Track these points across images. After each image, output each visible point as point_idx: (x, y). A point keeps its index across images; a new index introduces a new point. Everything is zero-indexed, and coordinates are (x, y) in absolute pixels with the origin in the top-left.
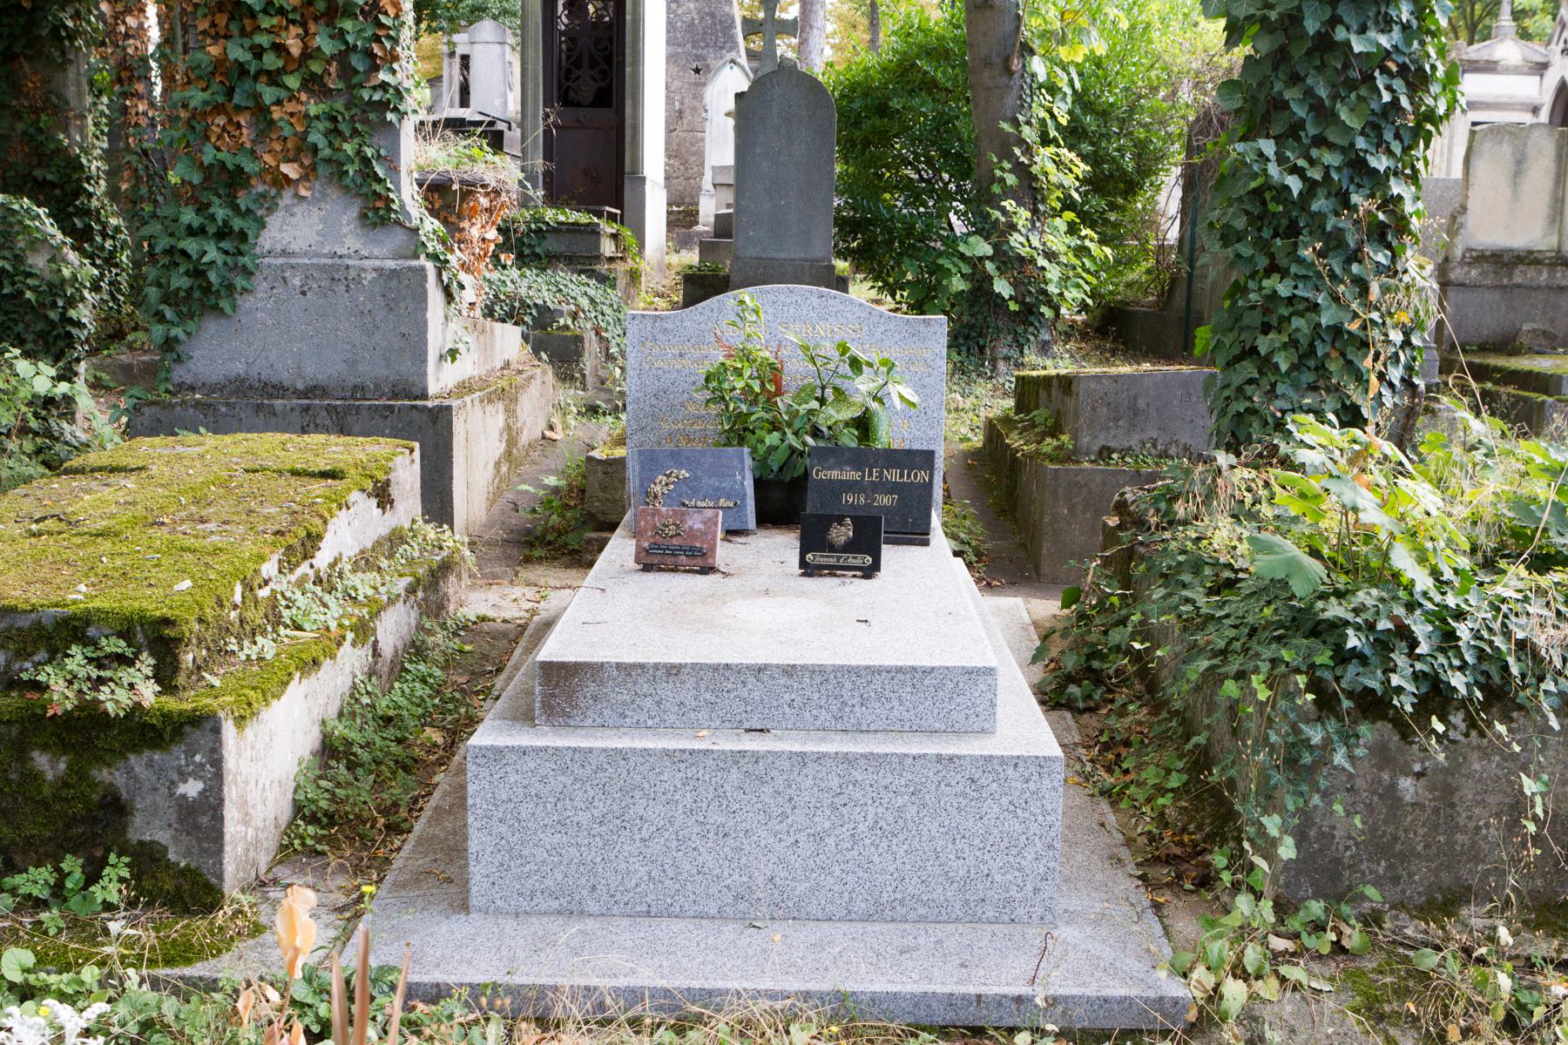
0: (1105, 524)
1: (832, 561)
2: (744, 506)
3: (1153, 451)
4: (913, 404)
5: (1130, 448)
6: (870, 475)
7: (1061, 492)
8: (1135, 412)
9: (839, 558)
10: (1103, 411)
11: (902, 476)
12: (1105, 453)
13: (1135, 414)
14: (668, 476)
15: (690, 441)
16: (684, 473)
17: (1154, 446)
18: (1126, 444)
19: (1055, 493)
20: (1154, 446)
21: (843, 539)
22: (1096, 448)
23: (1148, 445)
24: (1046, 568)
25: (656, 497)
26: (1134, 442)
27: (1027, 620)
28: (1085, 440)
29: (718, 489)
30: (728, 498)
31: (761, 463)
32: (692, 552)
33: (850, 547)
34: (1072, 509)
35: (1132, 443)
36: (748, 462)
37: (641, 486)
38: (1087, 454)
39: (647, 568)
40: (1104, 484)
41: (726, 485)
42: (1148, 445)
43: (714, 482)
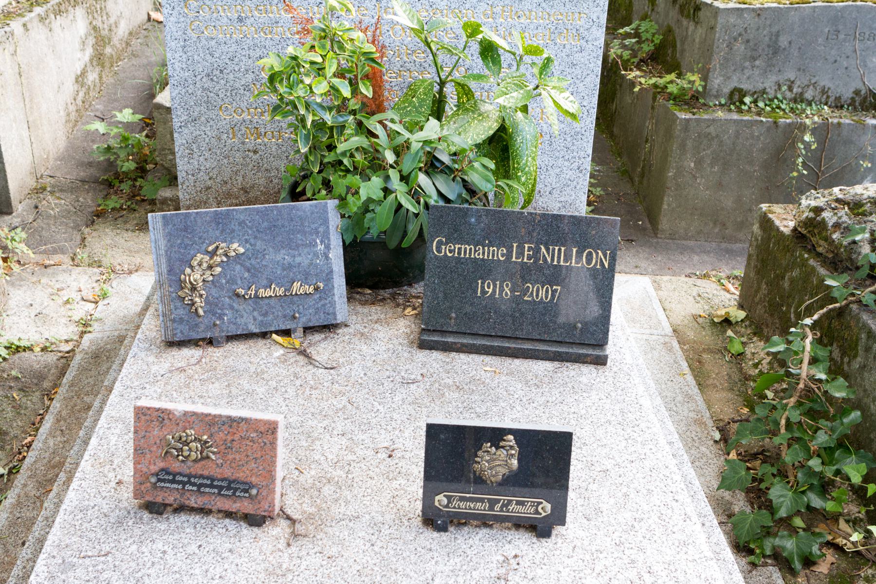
0: (766, 223)
1: (481, 508)
2: (329, 290)
3: (789, 95)
4: (573, 116)
5: (764, 91)
6: (520, 254)
7: (689, 143)
8: (775, 50)
9: (492, 503)
10: (740, 47)
11: (568, 258)
12: (736, 97)
13: (775, 53)
14: (213, 254)
15: (259, 135)
16: (237, 247)
17: (790, 89)
18: (760, 86)
19: (683, 146)
20: (790, 89)
21: (503, 471)
22: (727, 90)
23: (784, 88)
24: (664, 223)
25: (194, 288)
26: (769, 84)
27: (669, 330)
28: (716, 81)
29: (290, 267)
30: (305, 281)
31: (355, 221)
32: (234, 487)
33: (516, 482)
34: (699, 162)
35: (767, 85)
36: (335, 221)
37: (170, 271)
38: (717, 97)
39: (155, 508)
40: (737, 135)
41: (303, 259)
42: (784, 88)
43: (284, 256)
